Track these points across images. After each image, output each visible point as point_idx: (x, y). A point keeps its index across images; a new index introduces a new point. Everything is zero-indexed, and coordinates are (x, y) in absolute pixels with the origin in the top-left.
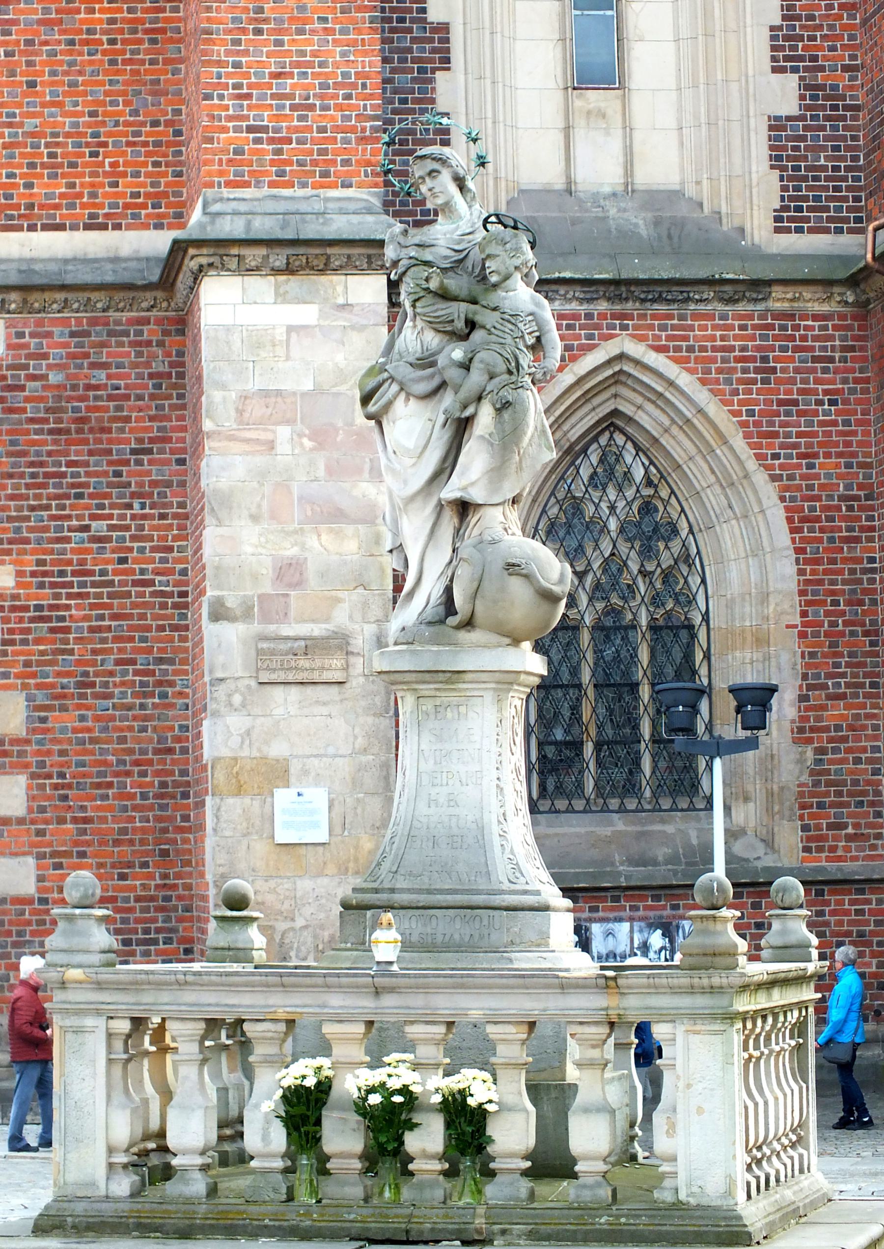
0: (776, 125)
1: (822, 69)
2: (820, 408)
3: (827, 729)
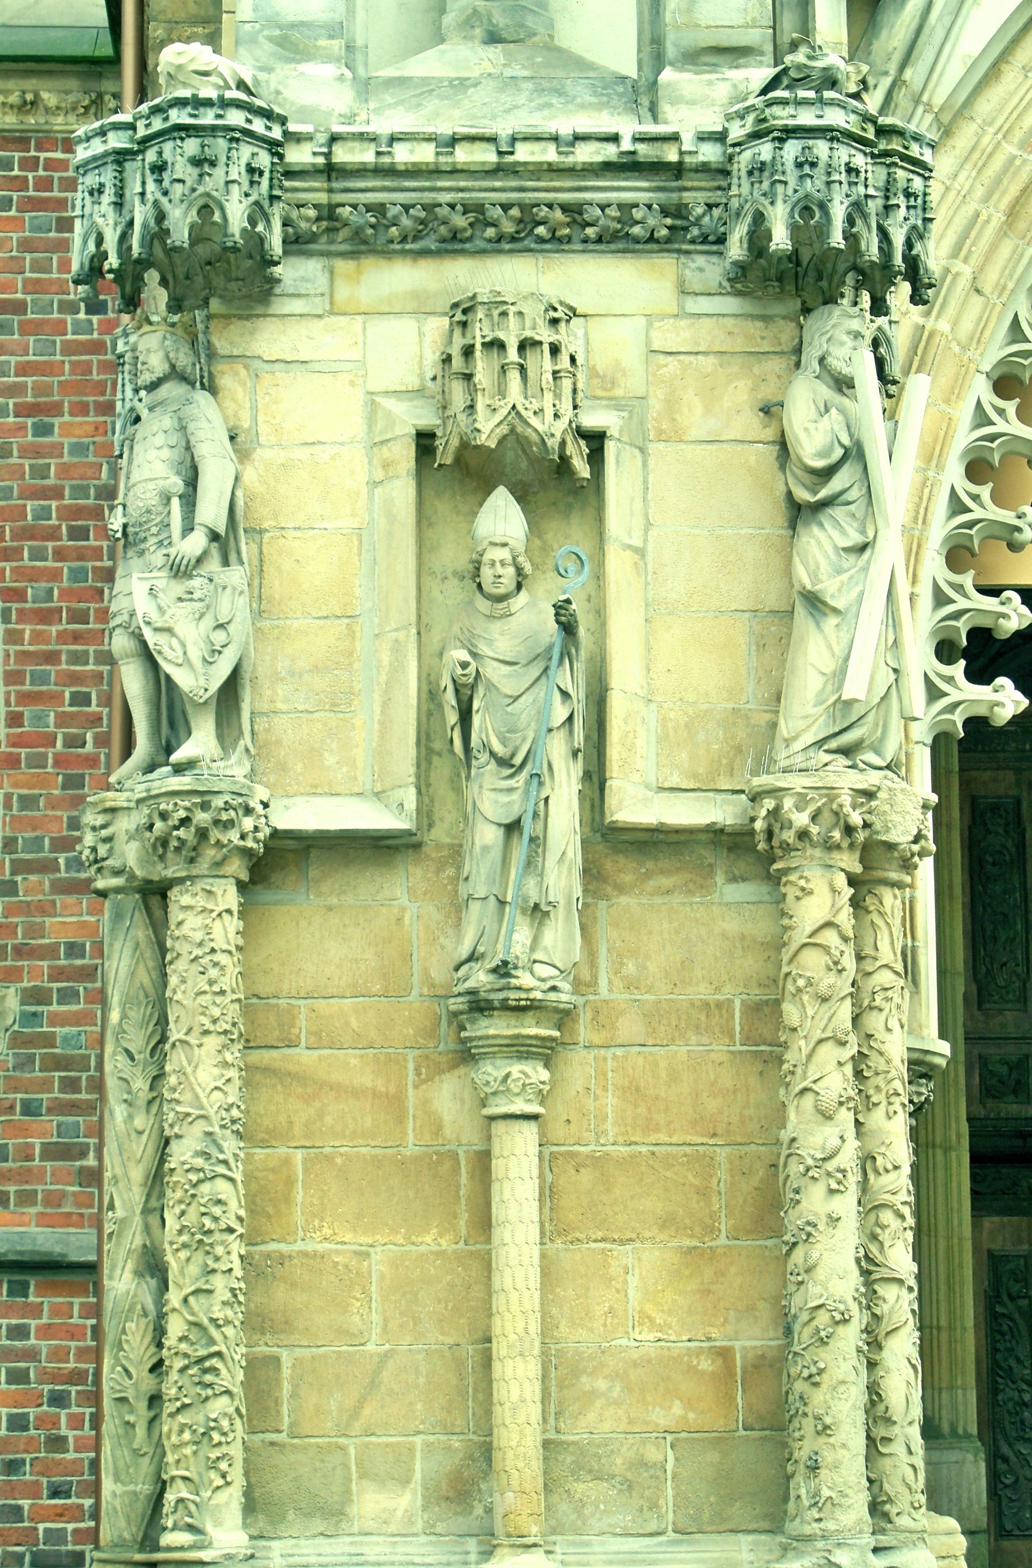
2: (69, 318)
3: (51, 952)
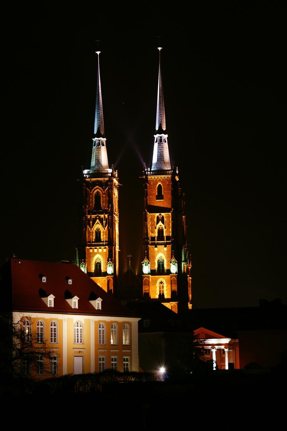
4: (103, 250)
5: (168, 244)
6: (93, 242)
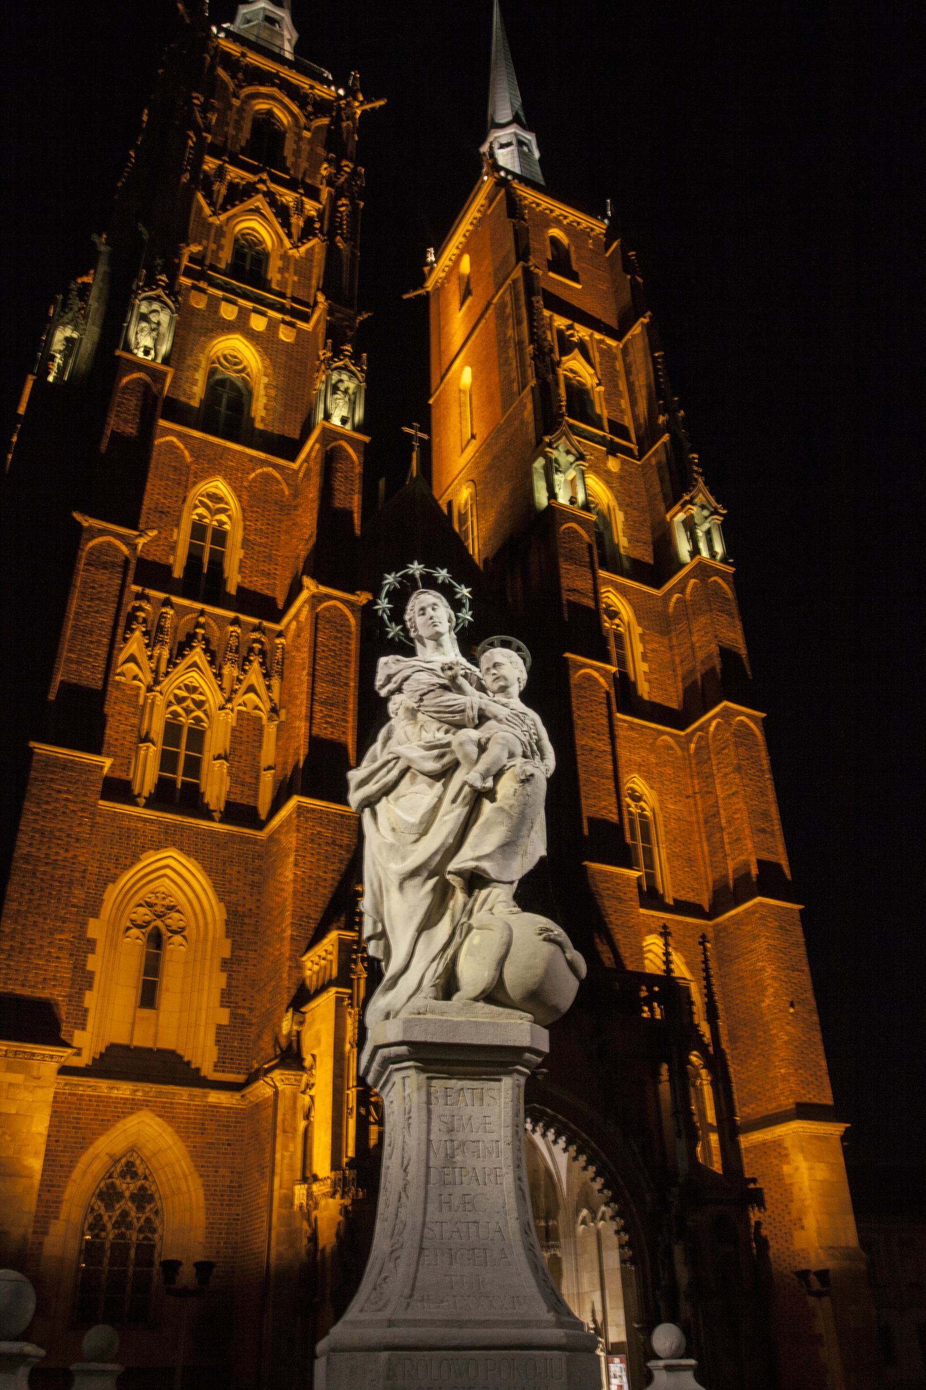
0: (219, 1027)
1: (239, 1007)
4: (272, 326)
5: (628, 452)
6: (213, 268)
